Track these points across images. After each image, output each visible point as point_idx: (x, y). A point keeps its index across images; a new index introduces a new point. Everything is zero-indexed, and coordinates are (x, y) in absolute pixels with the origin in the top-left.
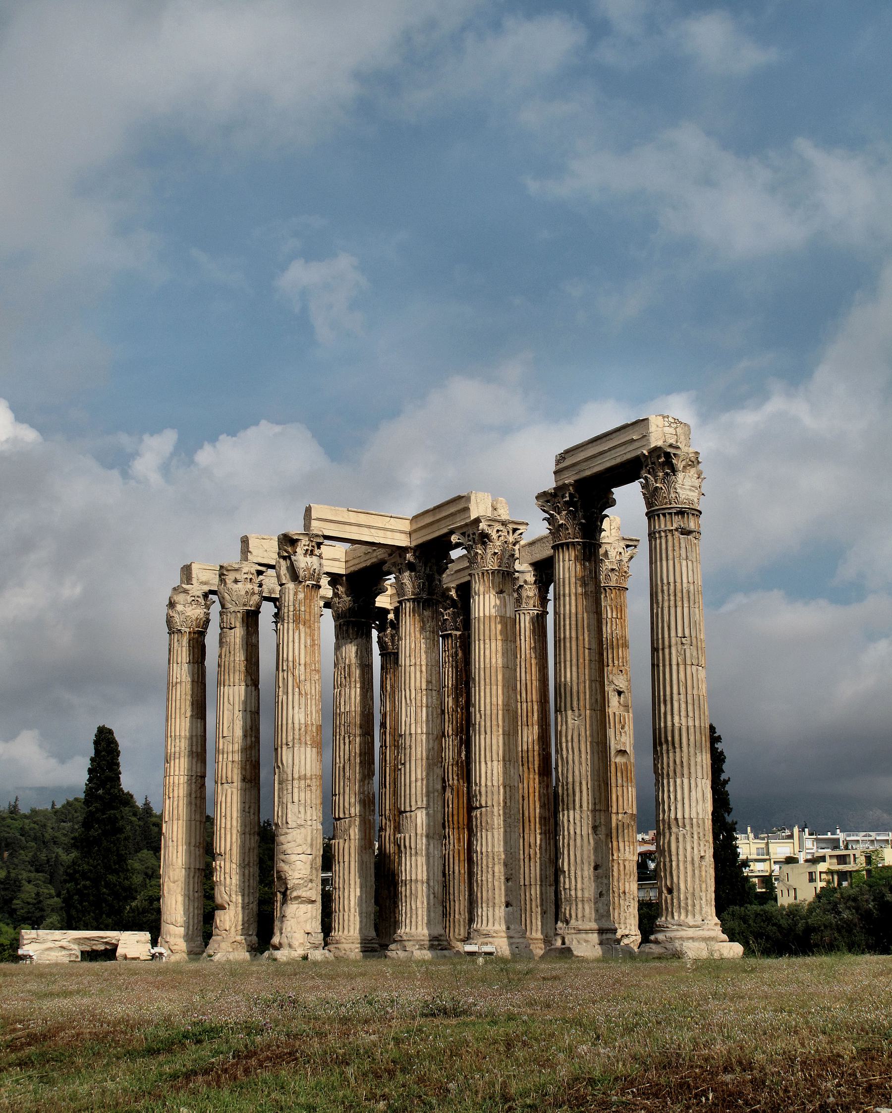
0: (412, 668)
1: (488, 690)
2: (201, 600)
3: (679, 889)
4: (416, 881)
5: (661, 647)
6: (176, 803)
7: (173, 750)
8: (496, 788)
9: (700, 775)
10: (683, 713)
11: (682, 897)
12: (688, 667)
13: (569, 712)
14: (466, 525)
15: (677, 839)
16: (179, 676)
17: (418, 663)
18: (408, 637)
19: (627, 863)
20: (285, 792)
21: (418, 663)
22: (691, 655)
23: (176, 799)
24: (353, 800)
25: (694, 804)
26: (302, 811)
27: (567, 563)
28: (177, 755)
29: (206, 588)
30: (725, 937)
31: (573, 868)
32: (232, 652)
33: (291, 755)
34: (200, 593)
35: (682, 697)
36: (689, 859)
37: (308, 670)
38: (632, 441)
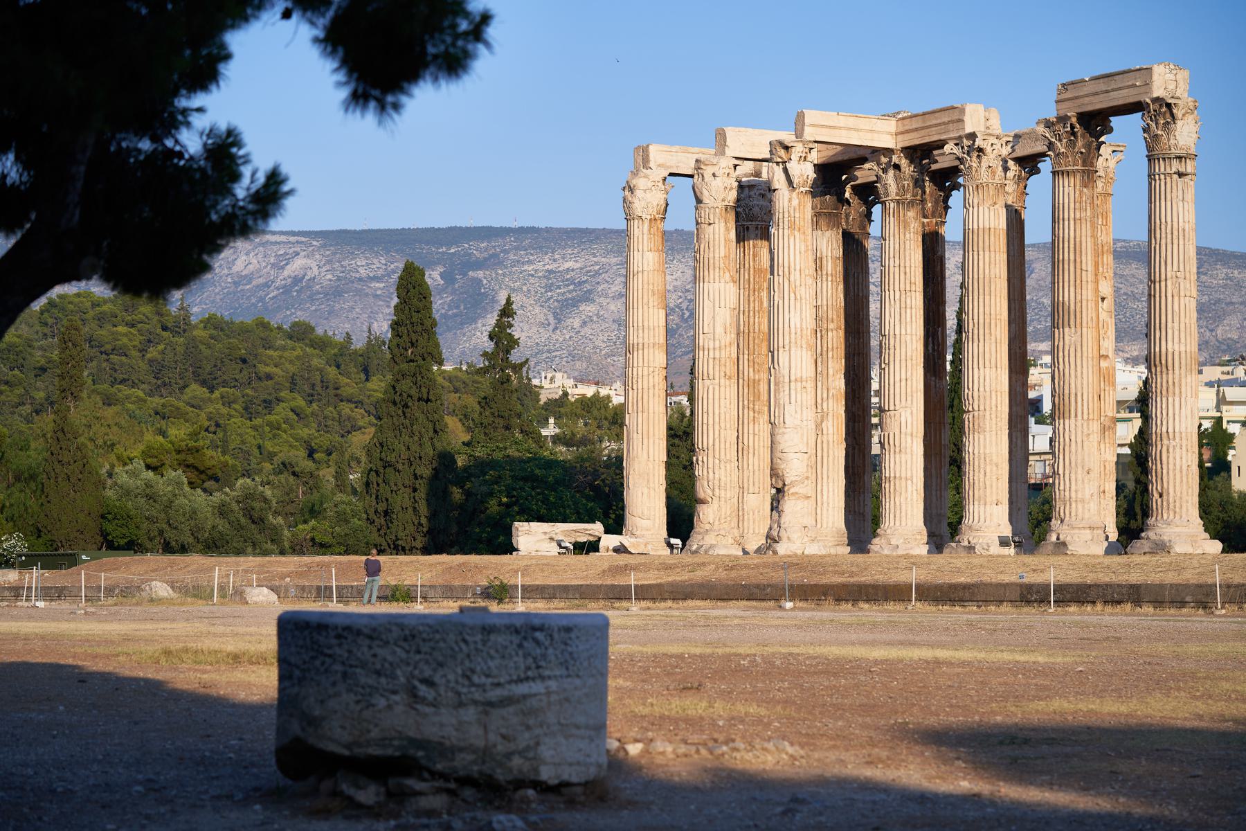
0: (897, 269)
1: (981, 300)
2: (661, 184)
3: (1168, 494)
4: (900, 478)
5: (1157, 279)
6: (640, 395)
7: (636, 342)
8: (988, 393)
9: (1189, 395)
10: (1176, 340)
11: (1171, 500)
12: (1182, 299)
13: (1067, 330)
14: (960, 138)
15: (1168, 450)
16: (640, 265)
17: (902, 265)
18: (892, 238)
19: (1107, 464)
20: (782, 394)
21: (902, 265)
22: (1185, 289)
23: (640, 391)
24: (825, 395)
25: (1183, 419)
26: (799, 412)
27: (1066, 189)
28: (640, 346)
29: (666, 174)
30: (1207, 536)
31: (1067, 472)
32: (712, 249)
33: (787, 360)
34: (660, 178)
35: (1176, 325)
36: (1178, 467)
37: (803, 276)
38: (1136, 86)
